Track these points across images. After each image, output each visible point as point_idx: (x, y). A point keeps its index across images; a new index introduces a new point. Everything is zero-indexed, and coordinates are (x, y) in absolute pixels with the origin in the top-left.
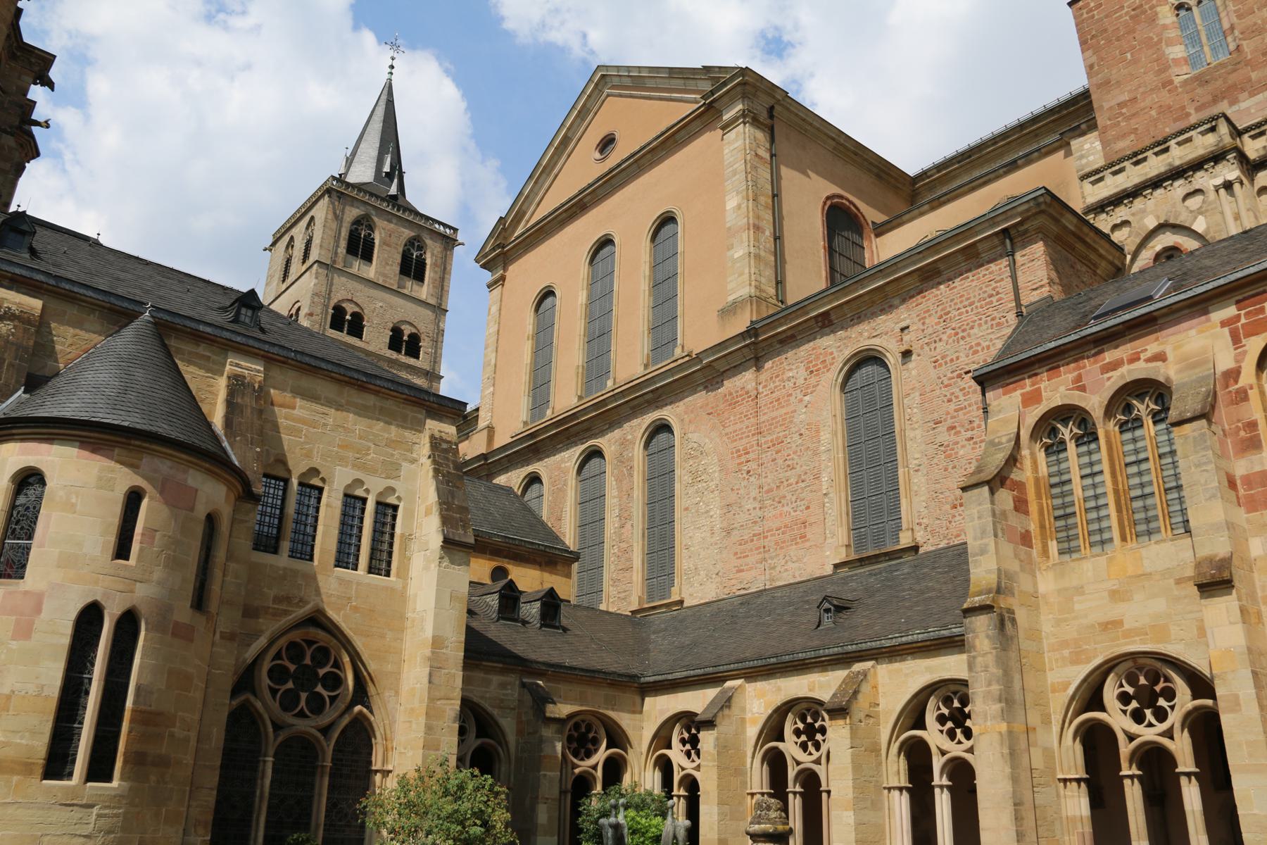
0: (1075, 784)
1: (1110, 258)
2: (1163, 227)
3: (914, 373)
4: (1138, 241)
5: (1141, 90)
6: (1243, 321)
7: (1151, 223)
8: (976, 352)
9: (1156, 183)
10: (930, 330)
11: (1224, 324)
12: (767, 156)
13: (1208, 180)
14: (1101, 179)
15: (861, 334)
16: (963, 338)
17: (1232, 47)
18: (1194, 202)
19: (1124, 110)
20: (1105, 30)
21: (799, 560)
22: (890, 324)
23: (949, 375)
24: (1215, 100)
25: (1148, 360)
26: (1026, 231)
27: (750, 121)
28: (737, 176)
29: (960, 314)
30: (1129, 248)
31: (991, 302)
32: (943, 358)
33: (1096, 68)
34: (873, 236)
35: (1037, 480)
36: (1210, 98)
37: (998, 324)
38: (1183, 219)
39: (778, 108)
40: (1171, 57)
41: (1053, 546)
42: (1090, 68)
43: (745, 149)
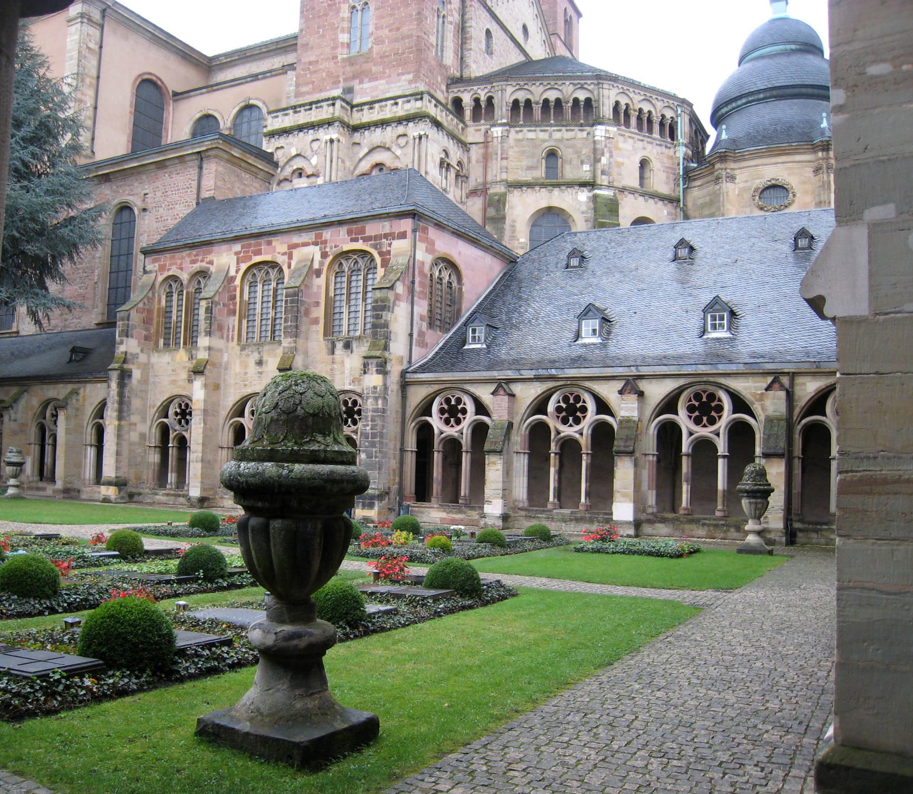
0: (153, 449)
1: (266, 170)
2: (298, 155)
3: (147, 222)
4: (285, 161)
5: (322, 57)
6: (242, 254)
7: (294, 152)
8: (176, 219)
9: (301, 128)
10: (157, 200)
11: (237, 253)
12: (96, 48)
13: (325, 135)
14: (277, 117)
15: (124, 192)
16: (171, 209)
17: (370, 45)
18: (315, 145)
19: (311, 67)
20: (314, 8)
21: (79, 318)
22: (139, 190)
23: (162, 228)
24: (354, 77)
25: (207, 263)
26: (209, 156)
27: (85, 20)
28: (73, 61)
29: (172, 194)
30: (281, 164)
31: (187, 192)
32: (161, 217)
33: (304, 32)
34: (171, 102)
35: (159, 309)
36: (351, 75)
37: (188, 206)
38: (308, 153)
39: (108, 11)
40: (341, 41)
41: (161, 342)
42: (301, 31)
43: (80, 43)
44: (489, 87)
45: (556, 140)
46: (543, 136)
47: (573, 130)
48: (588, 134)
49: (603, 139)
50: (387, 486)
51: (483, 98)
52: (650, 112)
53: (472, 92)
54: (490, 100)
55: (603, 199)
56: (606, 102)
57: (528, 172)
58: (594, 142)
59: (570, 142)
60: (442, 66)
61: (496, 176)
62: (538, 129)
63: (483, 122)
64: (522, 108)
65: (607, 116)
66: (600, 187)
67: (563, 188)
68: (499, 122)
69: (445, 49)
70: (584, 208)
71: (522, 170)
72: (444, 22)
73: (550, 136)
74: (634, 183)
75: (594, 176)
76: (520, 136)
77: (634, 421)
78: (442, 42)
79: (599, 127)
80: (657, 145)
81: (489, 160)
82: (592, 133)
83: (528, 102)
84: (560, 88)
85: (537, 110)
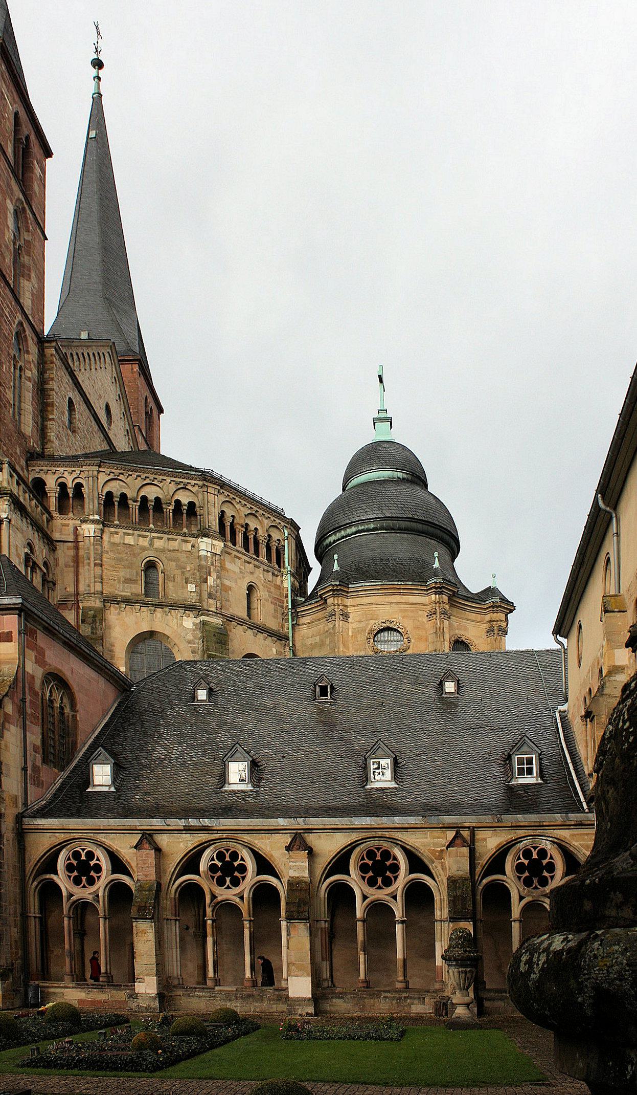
44: (78, 470)
45: (157, 550)
46: (144, 542)
47: (176, 540)
48: (193, 546)
49: (209, 554)
50: (9, 961)
51: (70, 485)
52: (256, 529)
53: (56, 476)
54: (79, 487)
55: (212, 627)
56: (212, 509)
57: (126, 585)
58: (199, 557)
59: (173, 554)
60: (21, 435)
61: (89, 586)
62: (136, 533)
63: (71, 515)
64: (116, 503)
65: (213, 527)
66: (207, 612)
67: (167, 610)
68: (91, 517)
69: (22, 412)
70: (190, 637)
71: (119, 582)
72: (21, 376)
73: (151, 544)
74: (243, 614)
75: (200, 601)
76: (116, 539)
77: (306, 883)
78: (20, 402)
79: (205, 539)
80: (264, 570)
81: (80, 564)
82: (196, 545)
83: (123, 496)
84: (160, 485)
85: (134, 506)
